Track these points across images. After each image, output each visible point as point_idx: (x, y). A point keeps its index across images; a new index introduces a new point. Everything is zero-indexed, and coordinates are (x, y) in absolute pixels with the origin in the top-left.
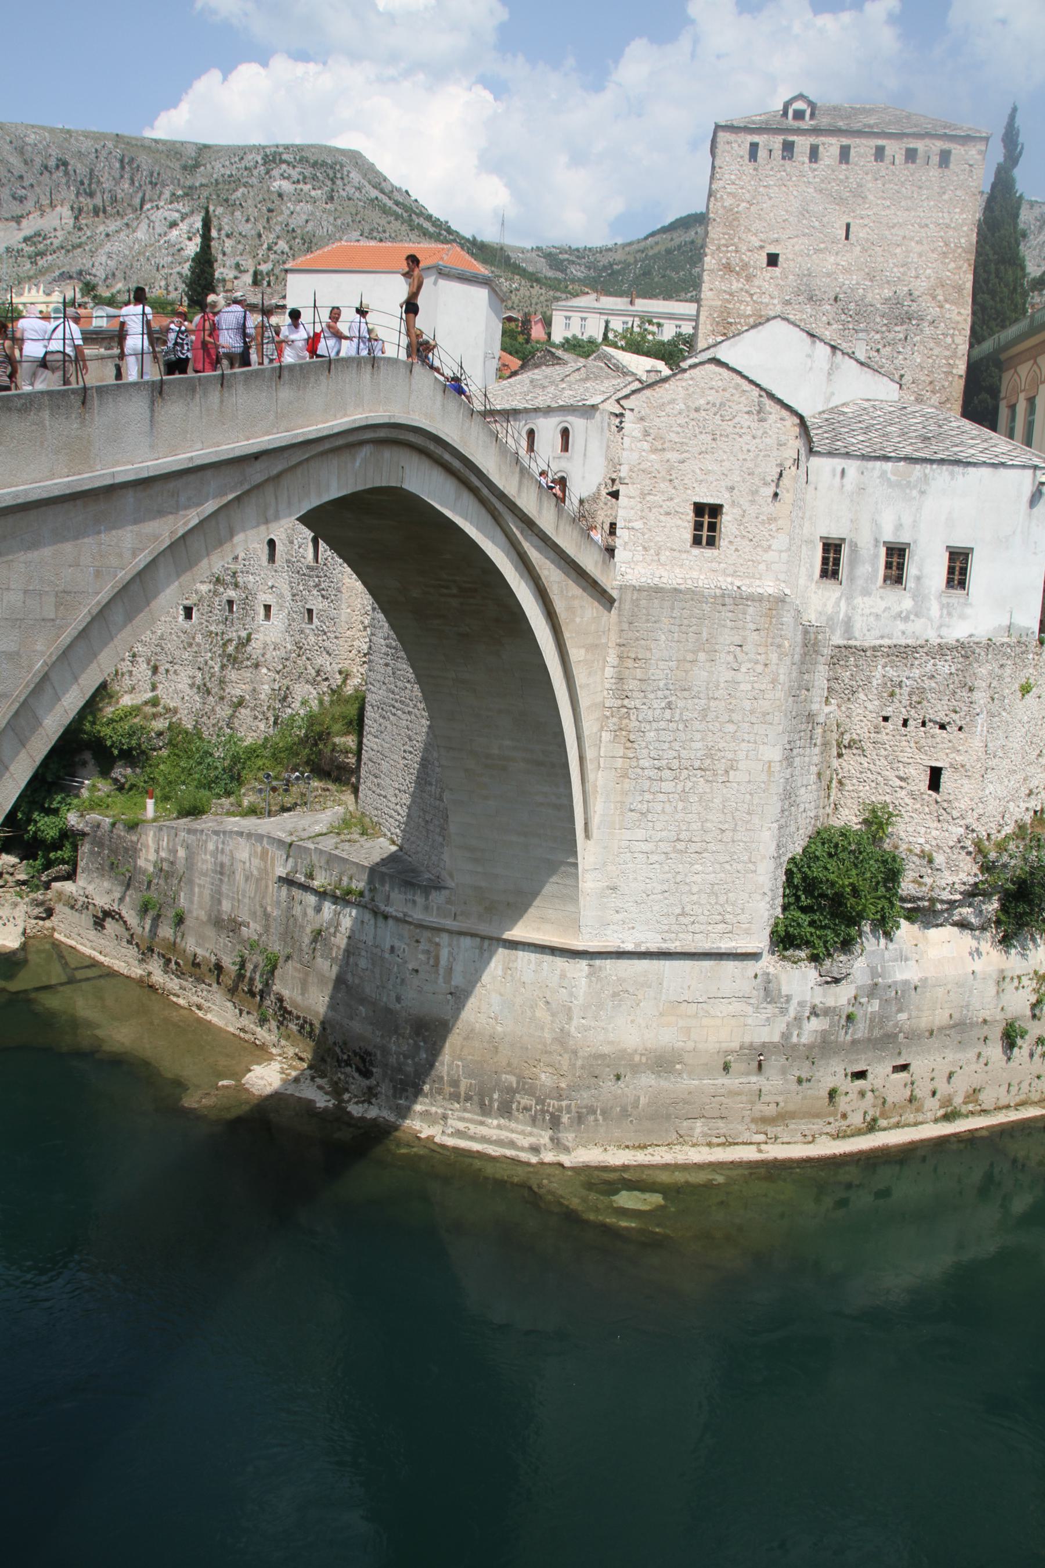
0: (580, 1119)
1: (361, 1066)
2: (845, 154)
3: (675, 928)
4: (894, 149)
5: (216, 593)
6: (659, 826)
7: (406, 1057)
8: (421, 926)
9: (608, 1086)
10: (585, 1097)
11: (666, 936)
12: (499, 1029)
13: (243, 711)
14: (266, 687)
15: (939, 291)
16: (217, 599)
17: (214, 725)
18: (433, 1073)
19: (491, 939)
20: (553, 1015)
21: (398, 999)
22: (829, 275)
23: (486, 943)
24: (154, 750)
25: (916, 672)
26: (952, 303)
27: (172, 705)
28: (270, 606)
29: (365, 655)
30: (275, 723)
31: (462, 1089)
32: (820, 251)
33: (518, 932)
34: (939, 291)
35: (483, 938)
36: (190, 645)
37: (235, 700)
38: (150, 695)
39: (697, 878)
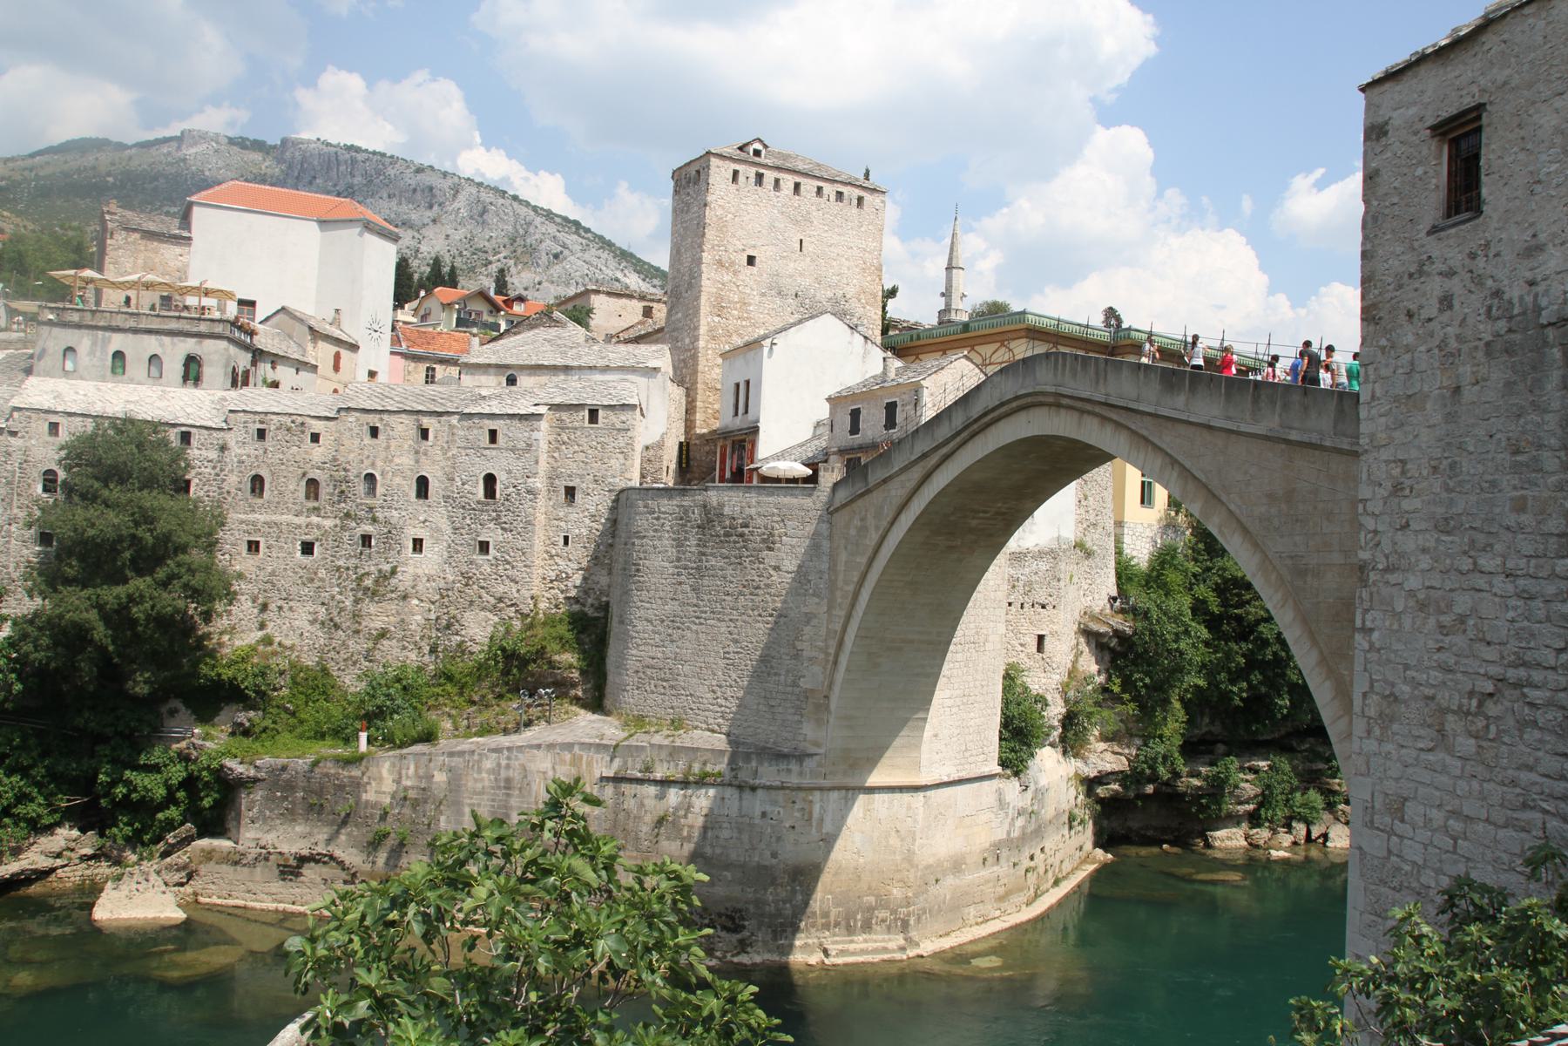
0: (919, 919)
1: (729, 924)
2: (797, 186)
3: (963, 761)
4: (829, 189)
5: (343, 528)
6: (956, 686)
7: (784, 902)
8: (799, 789)
9: (933, 890)
10: (921, 902)
11: (960, 767)
12: (861, 860)
13: (385, 642)
14: (418, 617)
15: (862, 296)
16: (347, 534)
17: (345, 660)
18: (809, 910)
19: (854, 789)
20: (902, 840)
21: (774, 855)
22: (791, 276)
23: (850, 792)
24: (275, 689)
25: (1027, 571)
26: (871, 306)
27: (288, 643)
28: (421, 540)
29: (552, 581)
30: (433, 650)
31: (832, 919)
32: (782, 257)
33: (874, 779)
34: (862, 296)
35: (847, 789)
36: (312, 580)
37: (374, 633)
38: (260, 634)
39: (972, 723)
